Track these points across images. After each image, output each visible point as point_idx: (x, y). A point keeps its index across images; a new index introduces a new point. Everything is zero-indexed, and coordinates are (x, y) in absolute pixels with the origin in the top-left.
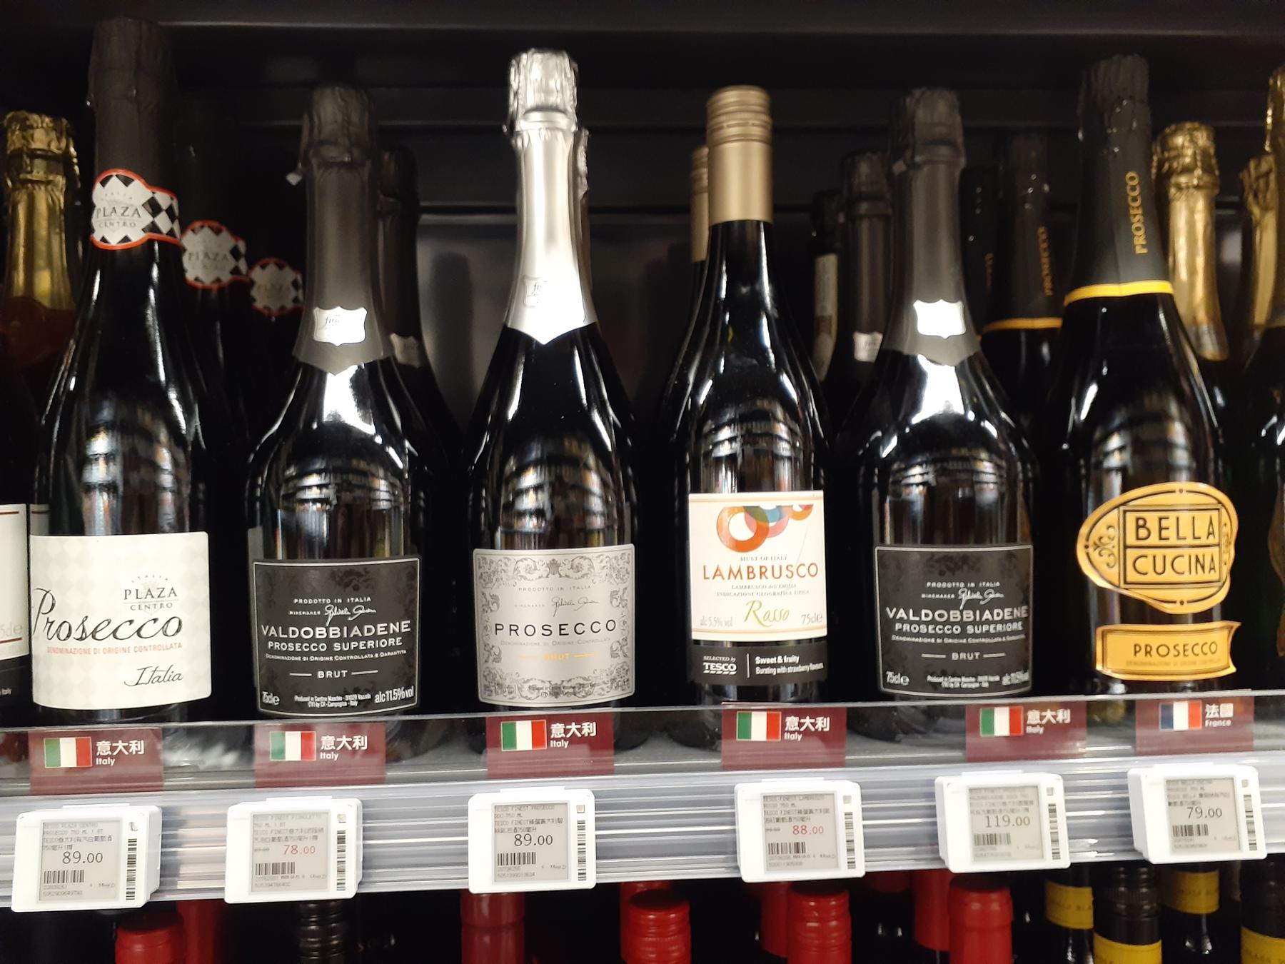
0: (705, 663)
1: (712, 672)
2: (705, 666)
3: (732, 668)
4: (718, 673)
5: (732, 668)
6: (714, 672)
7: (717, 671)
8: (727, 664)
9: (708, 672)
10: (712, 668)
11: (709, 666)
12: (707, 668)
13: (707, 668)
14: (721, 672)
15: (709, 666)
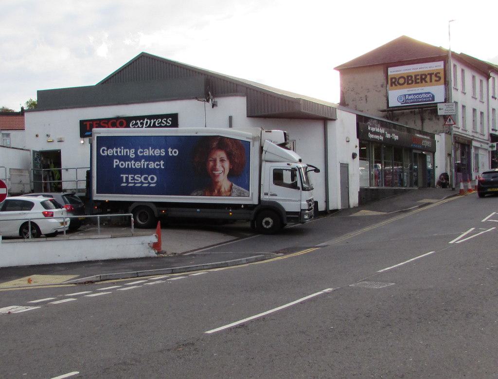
0: (121, 175)
1: (130, 185)
2: (123, 177)
3: (152, 179)
4: (137, 185)
5: (152, 179)
6: (132, 185)
7: (137, 183)
8: (147, 176)
9: (125, 185)
10: (130, 178)
11: (127, 178)
12: (124, 181)
13: (124, 181)
14: (139, 185)
15: (127, 178)
